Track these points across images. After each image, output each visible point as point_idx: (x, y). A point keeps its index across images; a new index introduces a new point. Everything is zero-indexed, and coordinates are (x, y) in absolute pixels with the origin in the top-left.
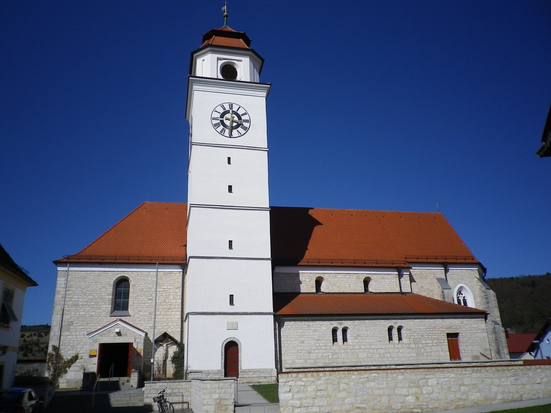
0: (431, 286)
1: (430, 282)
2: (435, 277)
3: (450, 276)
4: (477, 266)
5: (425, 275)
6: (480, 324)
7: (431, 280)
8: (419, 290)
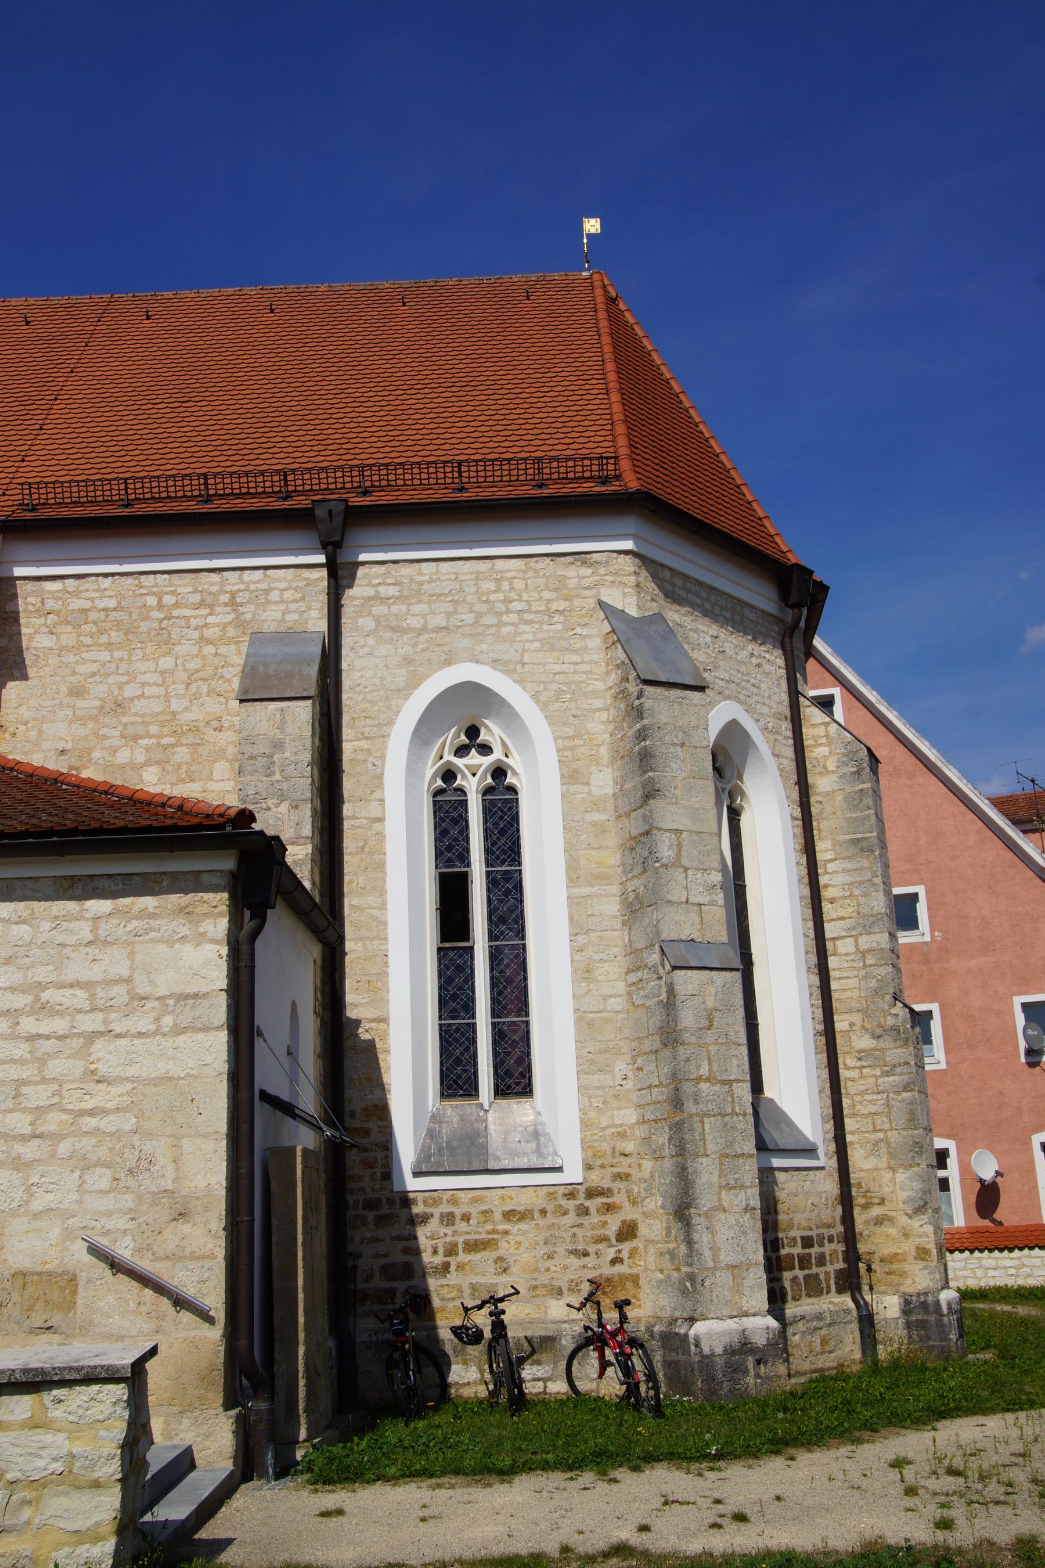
0: (197, 696)
1: (192, 665)
2: (239, 623)
3: (380, 610)
4: (631, 523)
5: (156, 614)
6: (169, 942)
7: (209, 649)
8: (82, 732)
